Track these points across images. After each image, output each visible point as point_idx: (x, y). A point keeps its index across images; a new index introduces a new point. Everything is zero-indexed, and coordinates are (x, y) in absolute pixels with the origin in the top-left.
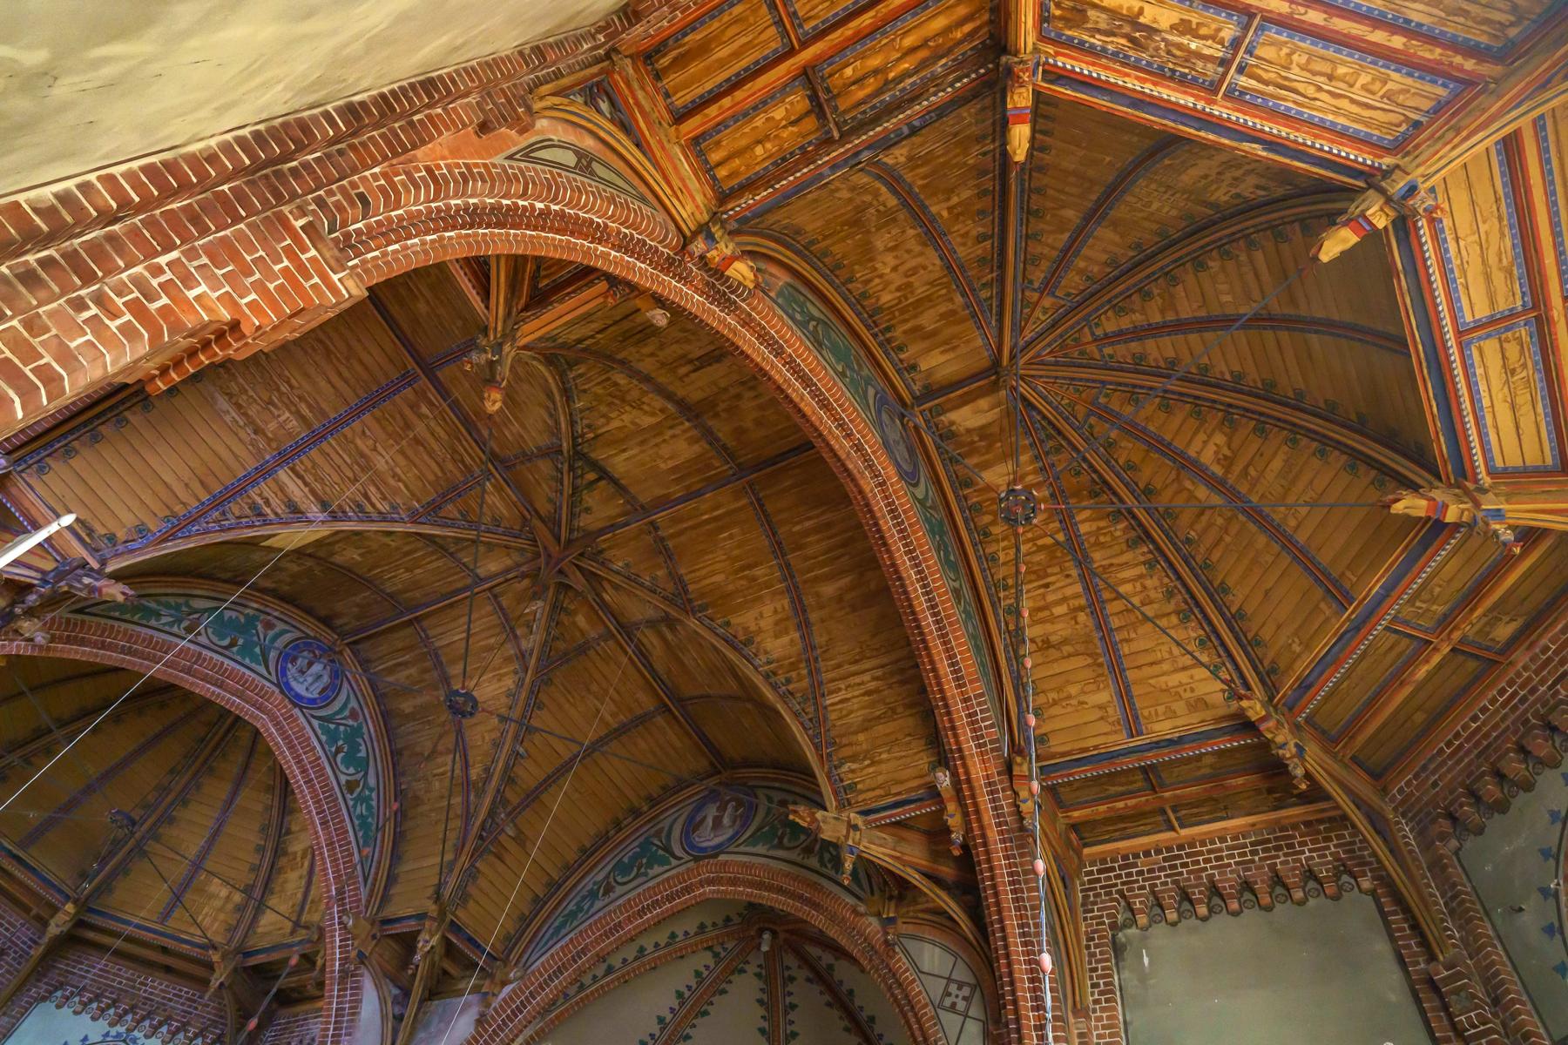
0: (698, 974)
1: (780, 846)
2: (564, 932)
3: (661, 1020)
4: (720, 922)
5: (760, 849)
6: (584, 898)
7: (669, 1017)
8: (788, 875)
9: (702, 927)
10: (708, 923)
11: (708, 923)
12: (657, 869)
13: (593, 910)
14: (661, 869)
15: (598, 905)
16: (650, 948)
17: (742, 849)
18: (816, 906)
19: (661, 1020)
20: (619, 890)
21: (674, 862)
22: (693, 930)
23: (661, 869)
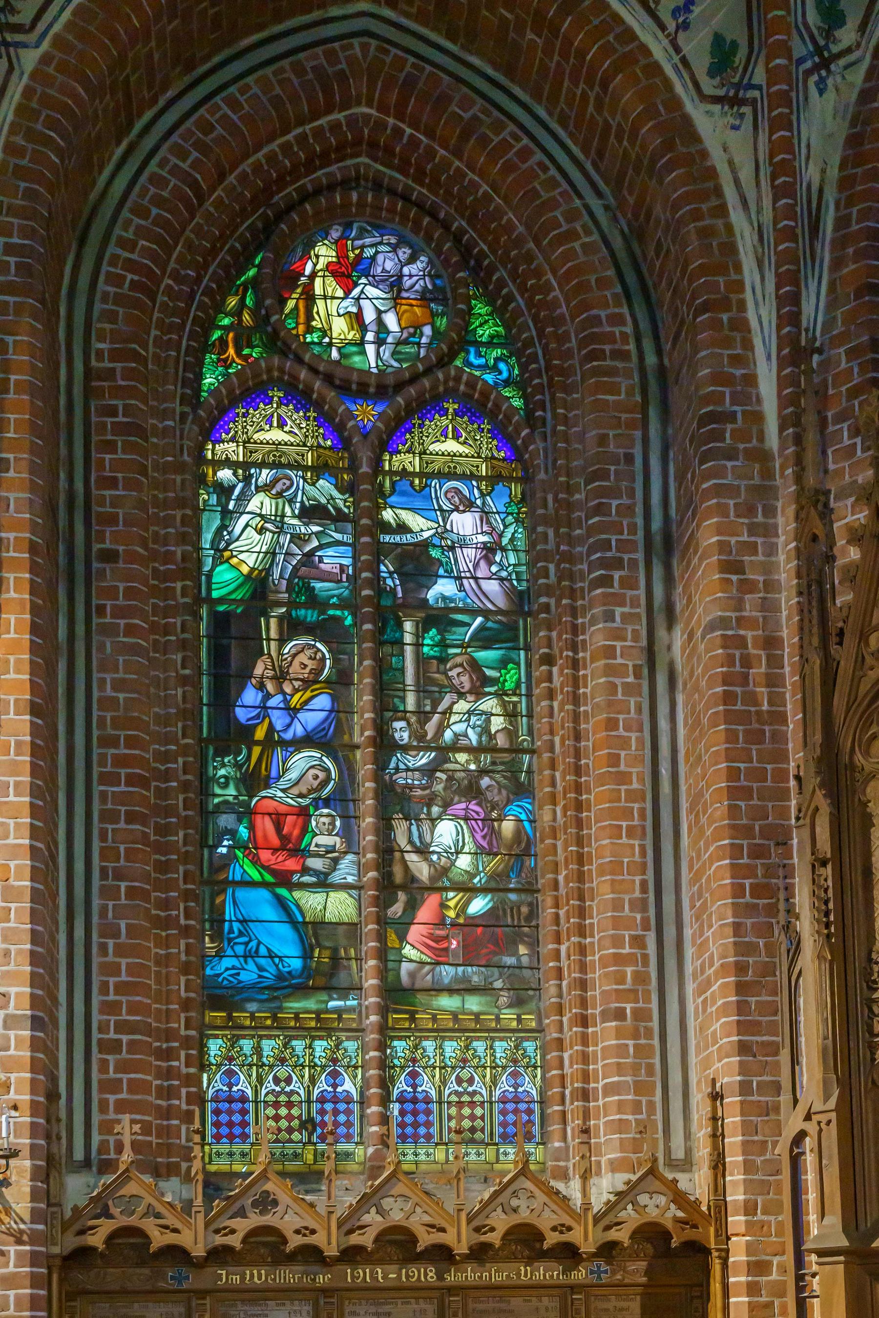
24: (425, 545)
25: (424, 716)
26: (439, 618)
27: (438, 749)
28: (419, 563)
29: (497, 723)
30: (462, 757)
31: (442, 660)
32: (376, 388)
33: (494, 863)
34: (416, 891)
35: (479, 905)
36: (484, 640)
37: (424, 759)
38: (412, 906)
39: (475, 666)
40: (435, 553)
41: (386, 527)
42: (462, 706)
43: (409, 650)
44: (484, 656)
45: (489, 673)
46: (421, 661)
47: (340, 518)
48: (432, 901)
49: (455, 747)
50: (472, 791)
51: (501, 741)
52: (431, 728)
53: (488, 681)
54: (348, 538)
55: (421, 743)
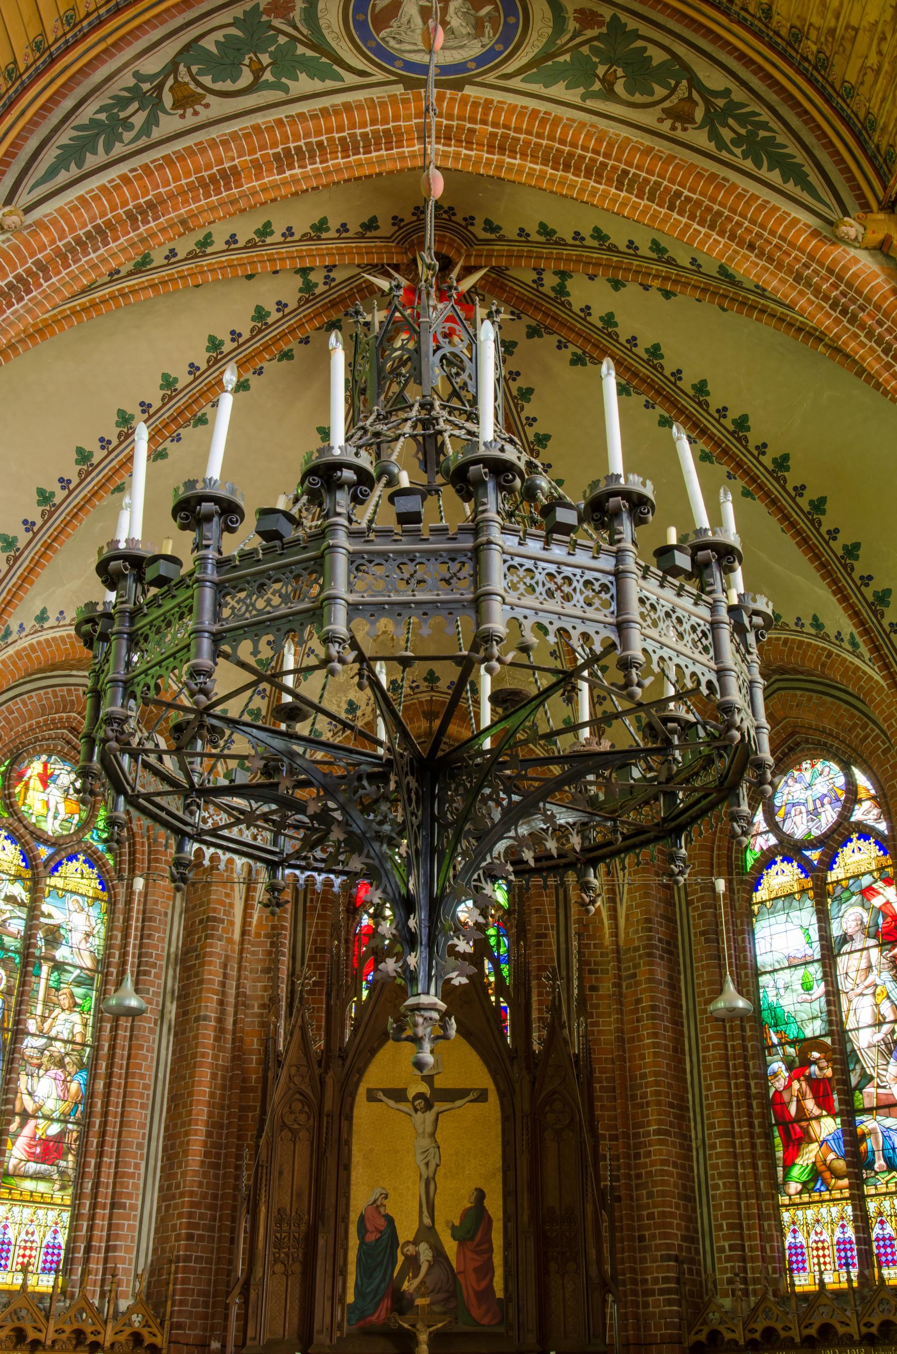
0: (260, 314)
1: (609, 93)
2: (91, 161)
3: (168, 382)
4: (354, 228)
5: (558, 90)
6: (121, 102)
7: (184, 379)
8: (649, 151)
9: (321, 226)
10: (334, 224)
11: (334, 224)
12: (304, 84)
13: (157, 134)
14: (318, 85)
15: (169, 124)
16: (219, 244)
17: (516, 83)
18: (713, 222)
19: (168, 382)
20: (218, 107)
21: (351, 79)
22: (301, 227)
23: (318, 85)
24: (59, 927)
25: (44, 1018)
26: (58, 967)
27: (49, 1038)
28: (54, 937)
29: (78, 1028)
30: (58, 1044)
31: (58, 990)
32: (53, 843)
33: (63, 1107)
34: (26, 1116)
35: (54, 1129)
36: (79, 983)
37: (41, 1042)
38: (22, 1126)
39: (72, 995)
40: (62, 932)
41: (43, 915)
42: (63, 1016)
43: (43, 982)
44: (79, 991)
45: (79, 1001)
46: (48, 988)
47: (22, 904)
48: (32, 1123)
49: (55, 1039)
50: (61, 1064)
51: (78, 1039)
52: (46, 1026)
53: (76, 1004)
54: (24, 916)
55: (41, 1034)
